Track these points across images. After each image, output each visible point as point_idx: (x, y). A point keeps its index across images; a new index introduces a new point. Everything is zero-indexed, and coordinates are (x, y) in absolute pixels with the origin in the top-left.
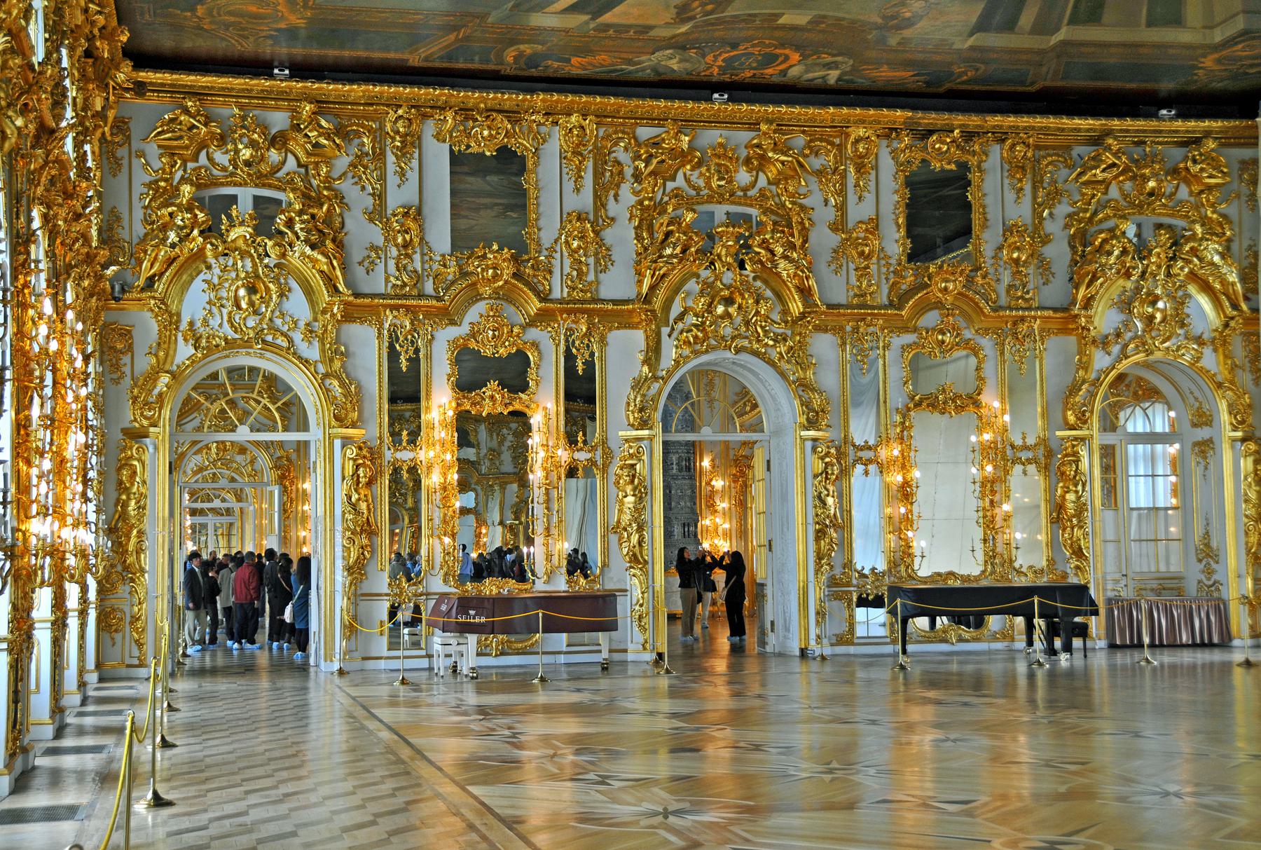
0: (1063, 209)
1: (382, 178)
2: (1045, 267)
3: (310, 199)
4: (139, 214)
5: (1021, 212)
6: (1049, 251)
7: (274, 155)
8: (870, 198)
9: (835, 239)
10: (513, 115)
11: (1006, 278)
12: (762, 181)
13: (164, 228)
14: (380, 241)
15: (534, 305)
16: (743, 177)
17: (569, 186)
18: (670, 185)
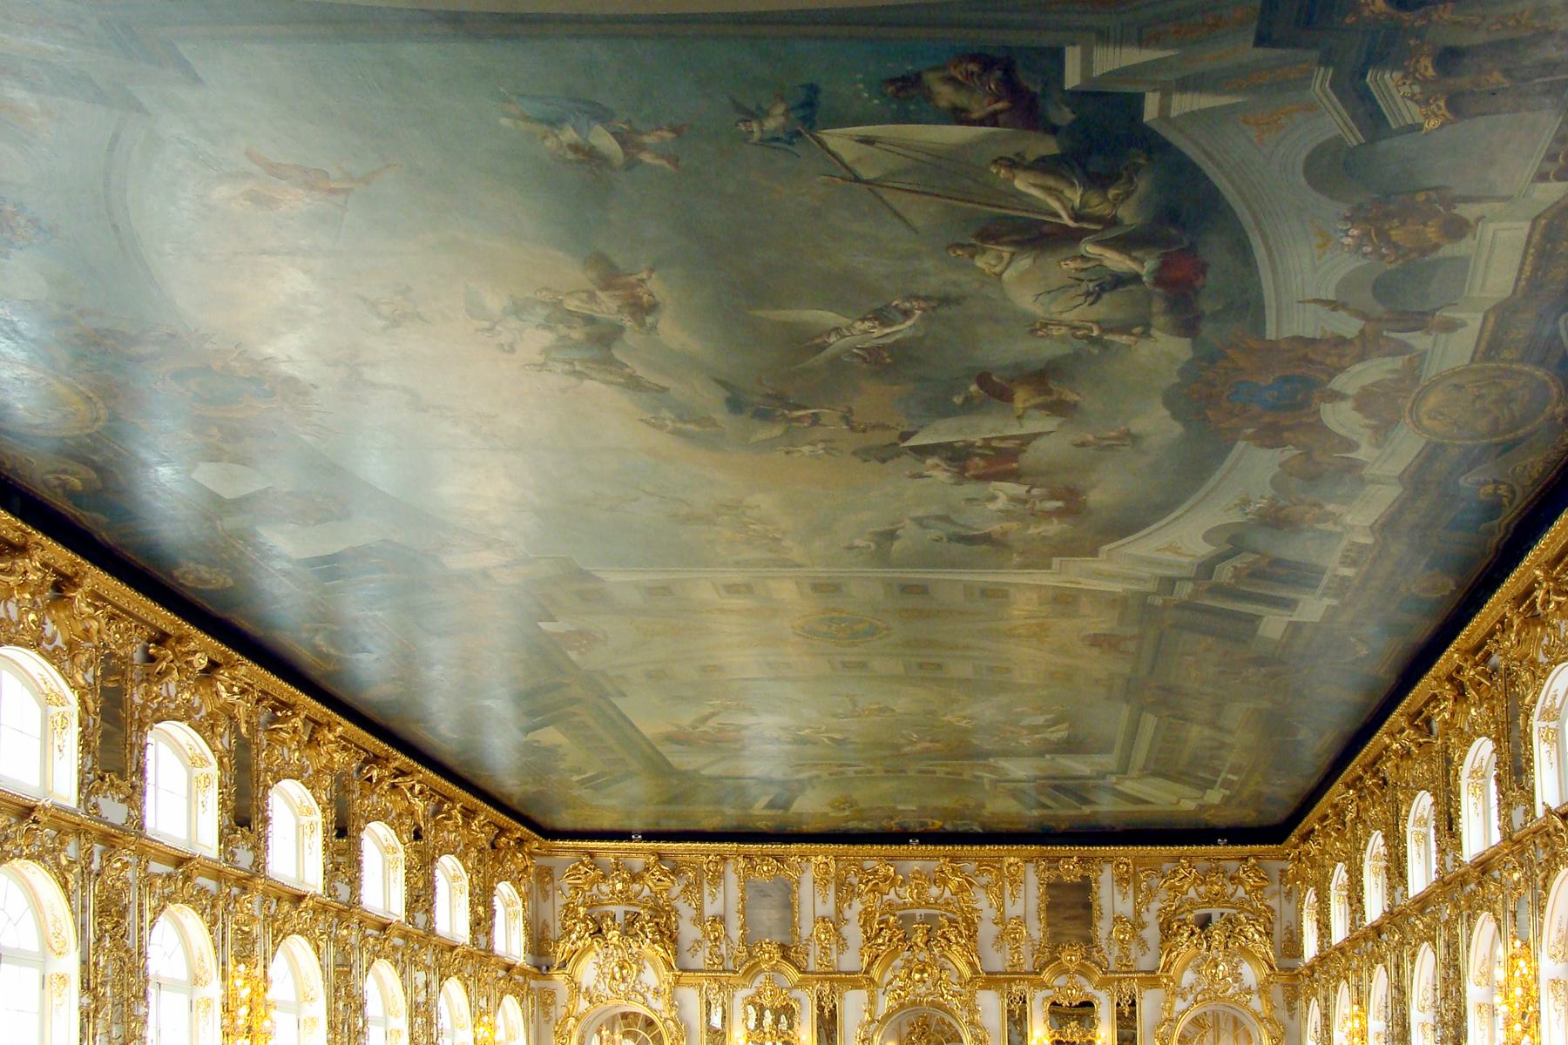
0: (1155, 905)
1: (701, 898)
2: (1143, 943)
3: (657, 911)
4: (559, 924)
5: (1125, 907)
6: (1146, 933)
7: (637, 887)
8: (1020, 902)
9: (995, 930)
10: (778, 858)
11: (1116, 952)
12: (947, 894)
13: (570, 932)
14: (700, 937)
15: (794, 975)
16: (934, 891)
17: (819, 900)
18: (886, 898)
